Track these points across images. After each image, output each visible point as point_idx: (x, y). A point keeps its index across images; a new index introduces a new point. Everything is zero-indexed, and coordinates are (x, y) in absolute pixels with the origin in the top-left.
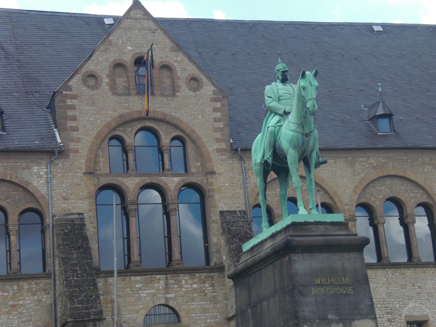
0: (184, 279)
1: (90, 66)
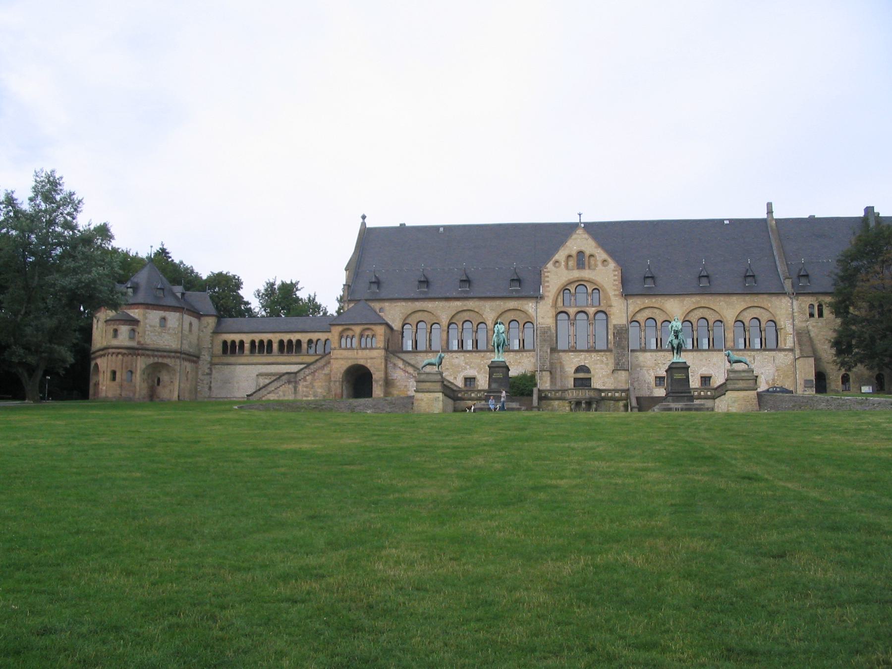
0: (593, 355)
1: (557, 257)
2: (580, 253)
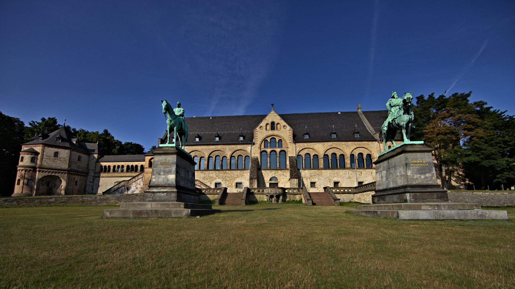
0: (279, 171)
1: (261, 125)
2: (273, 123)
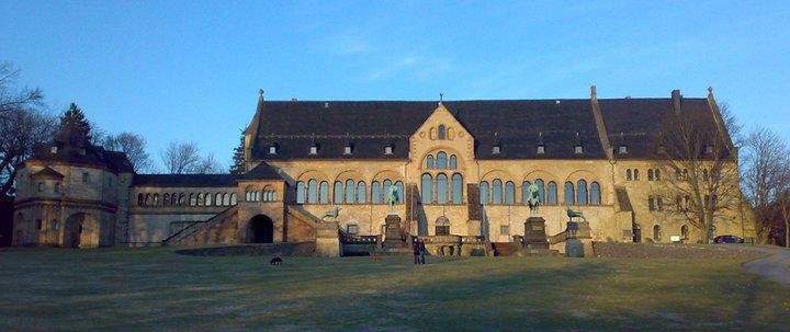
2: (442, 127)
